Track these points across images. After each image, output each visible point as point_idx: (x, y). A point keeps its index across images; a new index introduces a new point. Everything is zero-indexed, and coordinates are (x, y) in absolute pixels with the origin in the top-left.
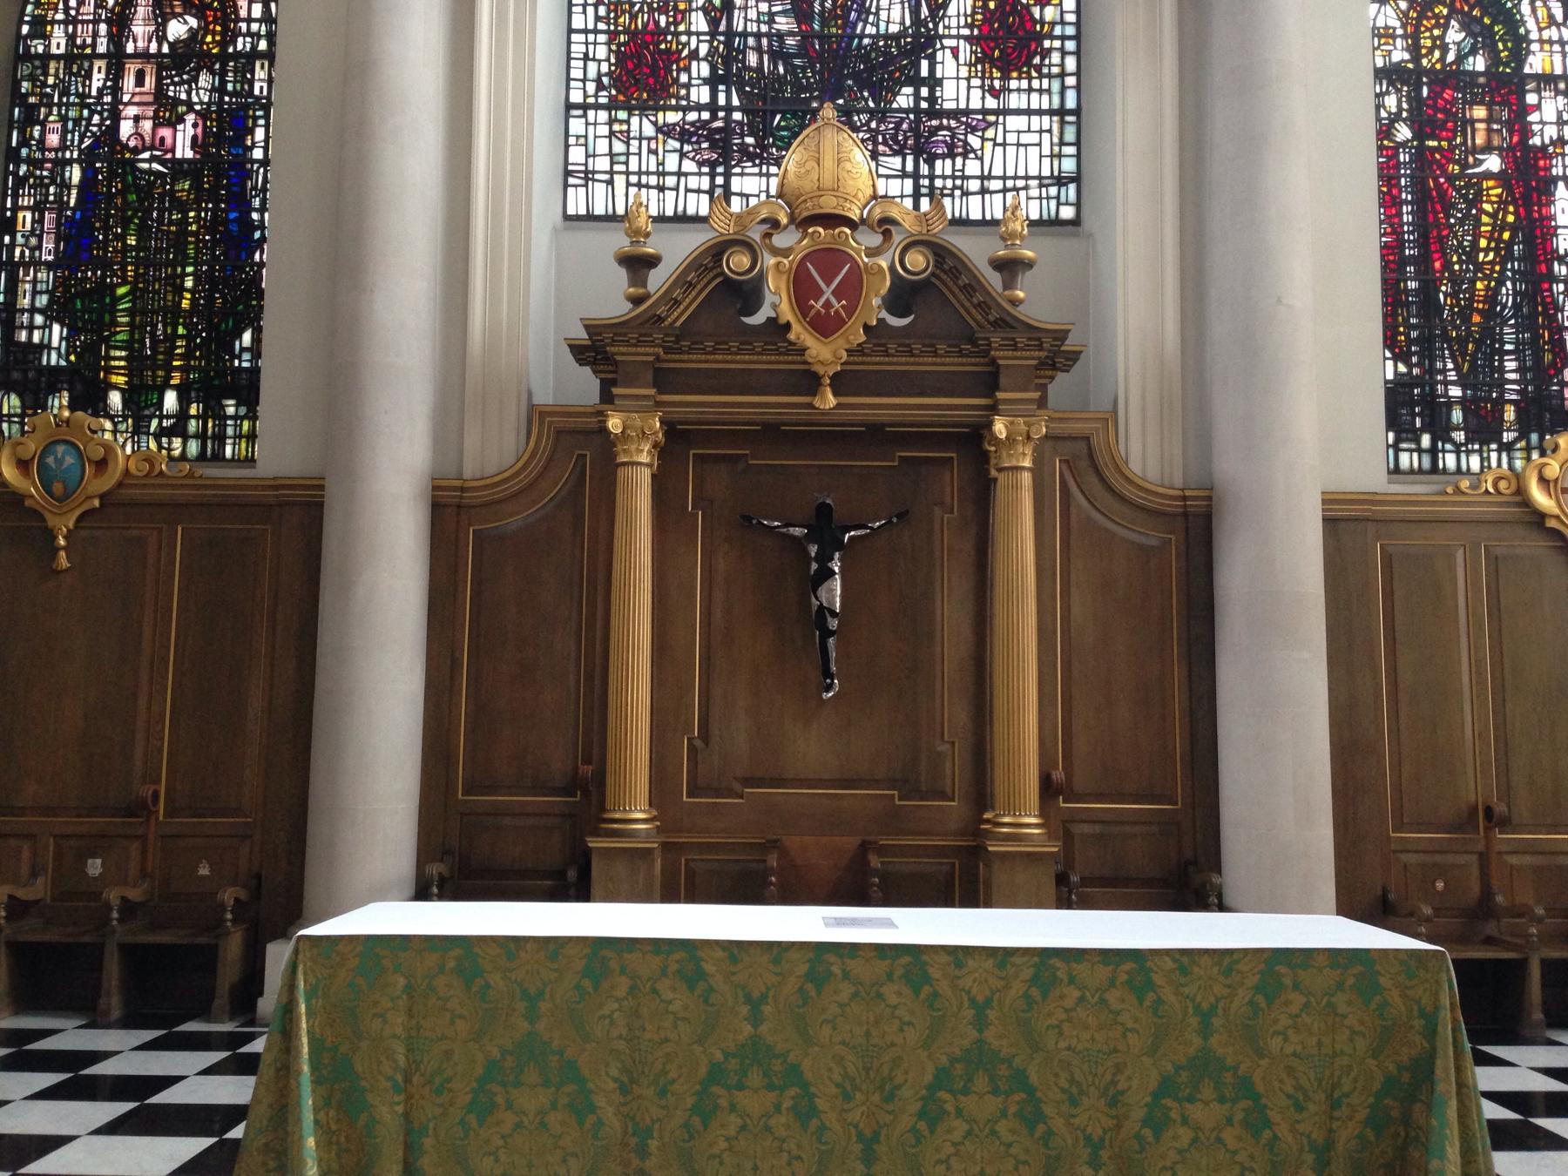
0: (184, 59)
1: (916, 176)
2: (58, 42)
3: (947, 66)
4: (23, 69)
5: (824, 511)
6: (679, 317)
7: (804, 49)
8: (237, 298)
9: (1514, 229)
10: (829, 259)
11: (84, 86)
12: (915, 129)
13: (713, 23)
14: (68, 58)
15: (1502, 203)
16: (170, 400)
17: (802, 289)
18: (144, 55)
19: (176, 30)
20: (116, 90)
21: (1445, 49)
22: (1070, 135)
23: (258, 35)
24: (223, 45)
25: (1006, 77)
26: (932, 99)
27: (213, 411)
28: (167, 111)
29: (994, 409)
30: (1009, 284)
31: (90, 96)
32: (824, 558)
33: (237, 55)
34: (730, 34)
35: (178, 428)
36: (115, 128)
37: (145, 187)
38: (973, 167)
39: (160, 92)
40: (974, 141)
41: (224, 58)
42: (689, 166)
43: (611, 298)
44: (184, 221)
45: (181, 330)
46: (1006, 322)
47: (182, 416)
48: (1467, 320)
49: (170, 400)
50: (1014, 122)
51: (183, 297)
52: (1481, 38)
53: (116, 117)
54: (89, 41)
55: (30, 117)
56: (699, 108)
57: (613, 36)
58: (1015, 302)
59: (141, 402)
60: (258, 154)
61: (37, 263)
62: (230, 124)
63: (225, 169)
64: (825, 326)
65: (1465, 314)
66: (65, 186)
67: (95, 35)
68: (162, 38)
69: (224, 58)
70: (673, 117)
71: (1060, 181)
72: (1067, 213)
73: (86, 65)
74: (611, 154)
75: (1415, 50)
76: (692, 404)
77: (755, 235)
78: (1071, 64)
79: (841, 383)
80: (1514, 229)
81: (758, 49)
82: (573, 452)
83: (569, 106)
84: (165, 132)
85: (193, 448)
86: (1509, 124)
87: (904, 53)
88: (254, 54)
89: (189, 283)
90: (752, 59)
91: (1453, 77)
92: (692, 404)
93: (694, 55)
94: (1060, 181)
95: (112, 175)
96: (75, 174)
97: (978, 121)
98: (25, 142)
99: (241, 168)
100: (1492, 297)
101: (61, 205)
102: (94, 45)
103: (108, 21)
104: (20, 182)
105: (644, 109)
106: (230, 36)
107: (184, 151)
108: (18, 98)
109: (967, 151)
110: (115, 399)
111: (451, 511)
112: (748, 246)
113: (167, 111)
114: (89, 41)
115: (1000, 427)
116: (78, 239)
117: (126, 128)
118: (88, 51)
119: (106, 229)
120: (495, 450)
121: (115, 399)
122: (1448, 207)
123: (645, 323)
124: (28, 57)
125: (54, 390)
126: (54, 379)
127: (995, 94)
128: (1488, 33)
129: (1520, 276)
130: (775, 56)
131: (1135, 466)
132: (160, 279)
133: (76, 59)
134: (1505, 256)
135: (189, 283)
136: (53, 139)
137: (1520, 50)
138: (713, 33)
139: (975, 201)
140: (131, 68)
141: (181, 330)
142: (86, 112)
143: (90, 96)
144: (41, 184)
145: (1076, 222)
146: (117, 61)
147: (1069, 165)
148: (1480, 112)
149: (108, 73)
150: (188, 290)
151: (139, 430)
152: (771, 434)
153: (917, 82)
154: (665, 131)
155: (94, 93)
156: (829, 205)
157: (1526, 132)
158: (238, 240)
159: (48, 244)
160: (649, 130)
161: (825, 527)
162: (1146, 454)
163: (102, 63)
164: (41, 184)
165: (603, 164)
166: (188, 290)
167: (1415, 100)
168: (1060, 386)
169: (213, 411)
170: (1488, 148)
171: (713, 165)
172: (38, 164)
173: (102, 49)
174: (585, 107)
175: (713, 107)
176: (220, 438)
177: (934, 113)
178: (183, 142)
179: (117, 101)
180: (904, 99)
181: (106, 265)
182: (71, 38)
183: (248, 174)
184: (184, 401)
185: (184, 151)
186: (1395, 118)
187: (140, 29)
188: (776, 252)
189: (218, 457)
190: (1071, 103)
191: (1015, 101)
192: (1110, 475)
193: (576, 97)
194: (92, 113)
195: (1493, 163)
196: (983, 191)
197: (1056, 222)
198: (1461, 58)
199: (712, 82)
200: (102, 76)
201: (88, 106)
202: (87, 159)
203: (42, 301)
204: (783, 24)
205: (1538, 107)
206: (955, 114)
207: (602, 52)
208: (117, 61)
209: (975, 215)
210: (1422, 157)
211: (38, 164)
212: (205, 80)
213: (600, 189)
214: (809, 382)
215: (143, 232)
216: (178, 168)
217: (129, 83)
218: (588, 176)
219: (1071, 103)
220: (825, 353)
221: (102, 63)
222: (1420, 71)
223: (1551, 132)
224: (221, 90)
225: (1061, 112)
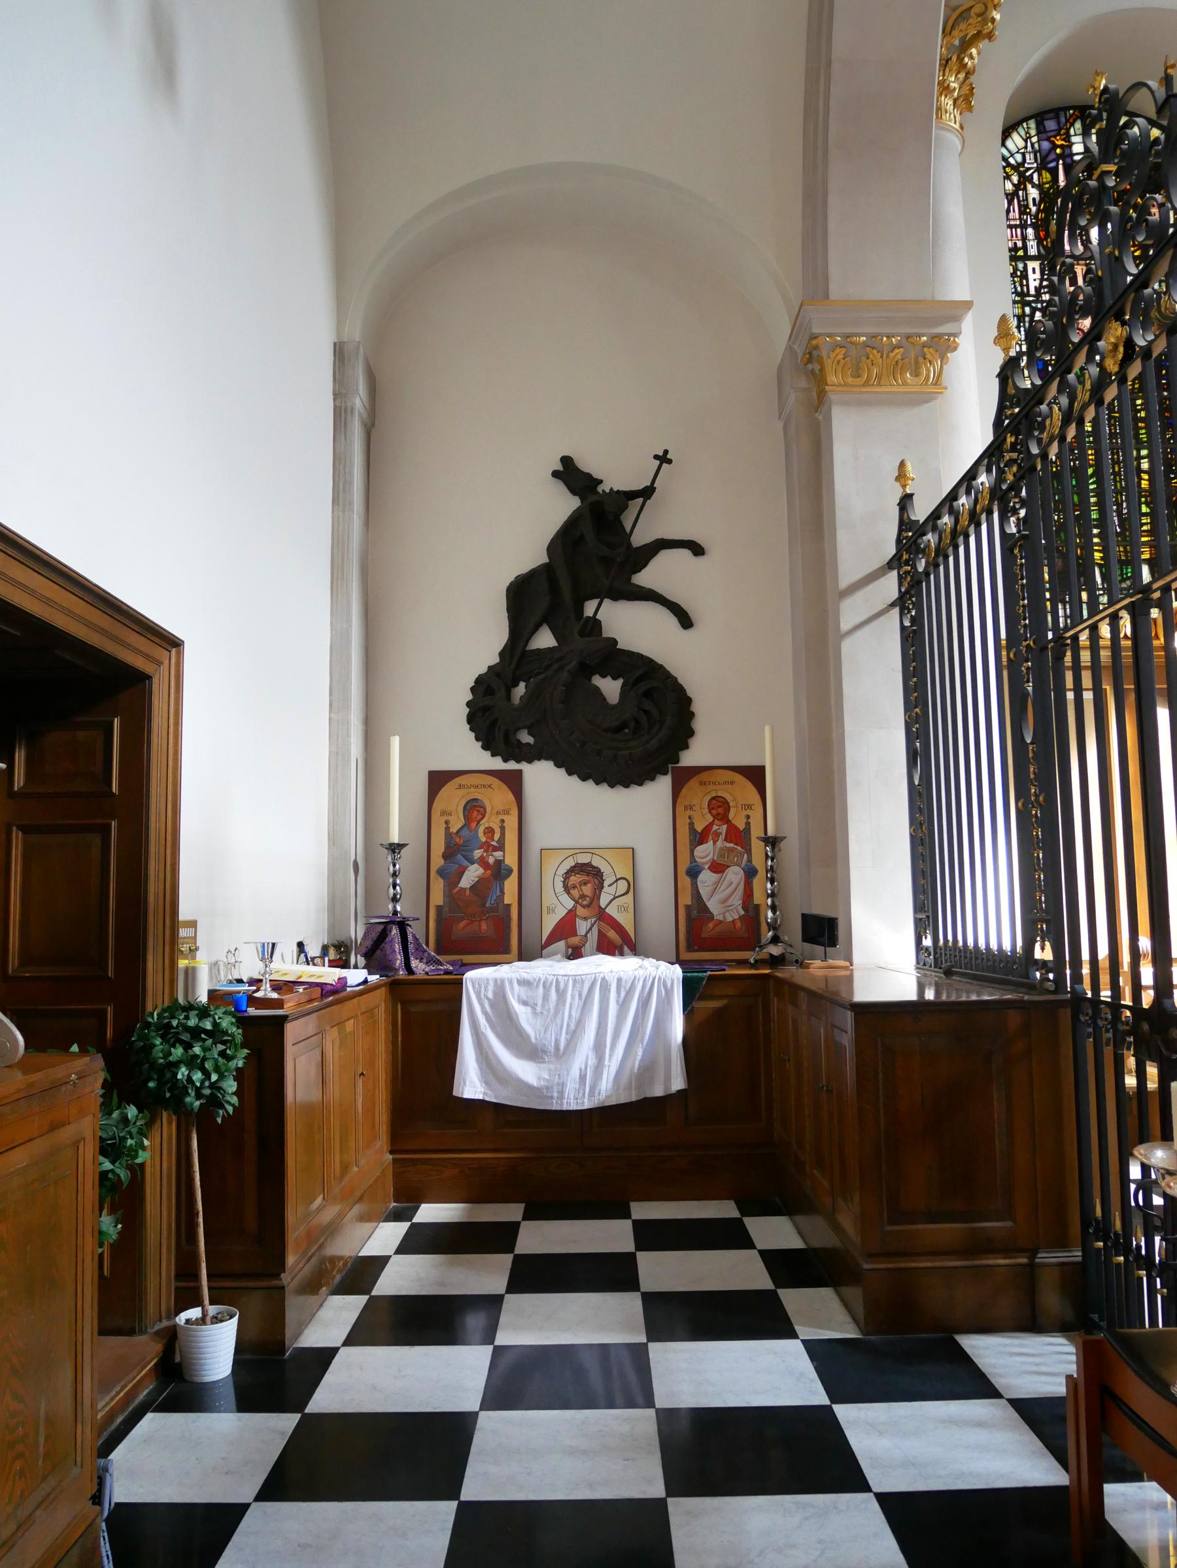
11: (1022, 285)
31: (1028, 295)
45: (1144, 509)
51: (1140, 479)
54: (1020, 244)
67: (1024, 238)
73: (1021, 266)
89: (1145, 465)
102: (1025, 248)
103: (1033, 225)
114: (1020, 244)
118: (1021, 253)
132: (1118, 462)
135: (1145, 465)
141: (1144, 509)
142: (1027, 310)
143: (1028, 295)
149: (1042, 274)
150: (1145, 472)
155: (1032, 292)
163: (1036, 264)
166: (1145, 472)
173: (1033, 251)
194: (1034, 310)
200: (1038, 275)
201: (1028, 304)
221: (1036, 264)
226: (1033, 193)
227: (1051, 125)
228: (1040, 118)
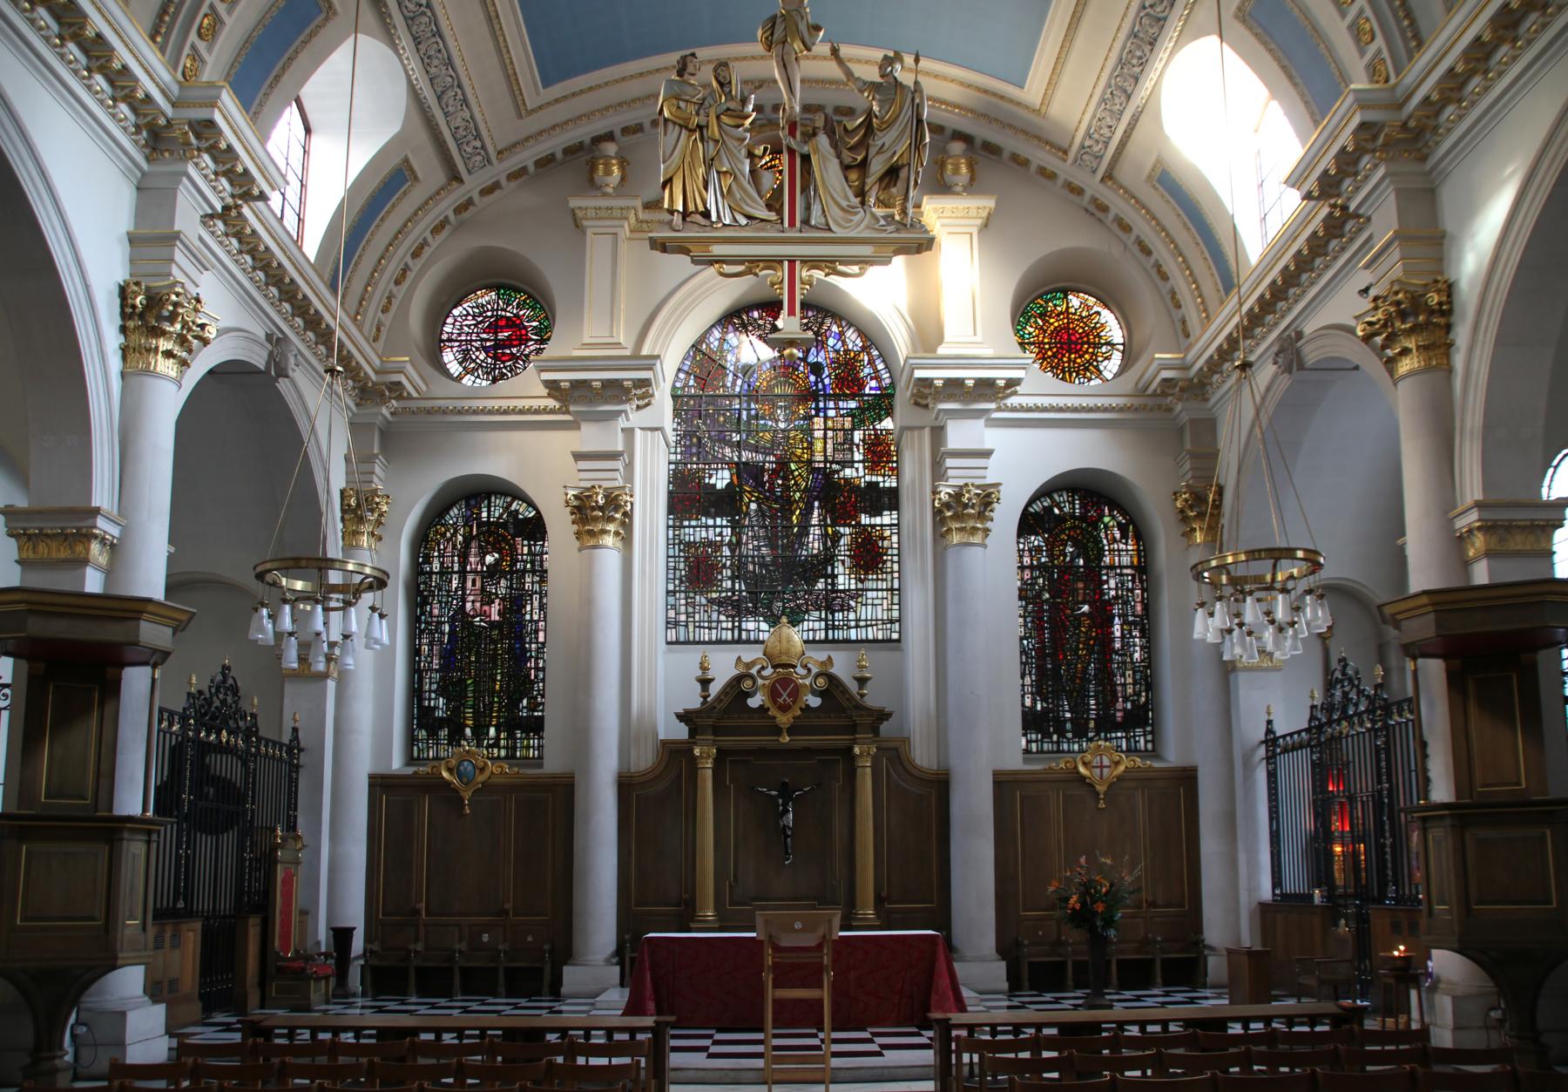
0: (493, 573)
1: (826, 620)
2: (436, 566)
3: (840, 569)
4: (422, 579)
5: (784, 785)
6: (722, 706)
7: (774, 562)
8: (521, 684)
9: (1095, 639)
10: (785, 682)
12: (826, 598)
13: (733, 551)
14: (441, 573)
15: (1090, 628)
16: (492, 731)
17: (774, 693)
18: (475, 572)
19: (489, 559)
20: (464, 589)
21: (1065, 555)
22: (896, 600)
23: (525, 562)
24: (511, 566)
25: (866, 573)
26: (833, 584)
27: (511, 736)
28: (487, 599)
29: (855, 741)
30: (861, 688)
32: (785, 805)
33: (517, 571)
34: (741, 556)
35: (496, 745)
36: (464, 606)
37: (478, 634)
38: (852, 616)
39: (483, 589)
40: (852, 603)
41: (512, 572)
42: (723, 618)
43: (695, 703)
44: (496, 649)
46: (859, 707)
47: (498, 738)
48: (1073, 682)
49: (492, 731)
50: (870, 594)
52: (1081, 550)
53: (464, 601)
55: (425, 602)
56: (727, 590)
57: (687, 558)
58: (862, 696)
59: (480, 732)
60: (528, 617)
61: (431, 670)
62: (515, 603)
63: (514, 626)
64: (784, 708)
65: (1073, 680)
66: (443, 633)
68: (483, 564)
69: (512, 572)
70: (714, 595)
71: (891, 622)
72: (895, 636)
74: (687, 613)
75: (1051, 556)
76: (729, 741)
77: (754, 671)
78: (896, 567)
79: (792, 731)
80: (1095, 639)
81: (754, 563)
82: (675, 756)
83: (668, 592)
84: (486, 608)
85: (503, 753)
86: (1094, 591)
87: (820, 563)
88: (525, 571)
90: (751, 567)
91: (1069, 568)
92: (729, 741)
93: (724, 566)
94: (891, 622)
95: (463, 628)
96: (447, 628)
97: (857, 594)
98: (423, 613)
99: (521, 624)
100: (1085, 670)
101: (442, 643)
104: (422, 632)
105: (701, 594)
106: (514, 562)
107: (495, 617)
108: (420, 593)
109: (849, 608)
110: (468, 731)
111: (626, 786)
112: (751, 677)
113: (487, 599)
115: (857, 750)
116: (447, 657)
117: (469, 606)
119: (461, 653)
120: (644, 760)
121: (468, 731)
122: (1066, 630)
123: (707, 709)
124: (422, 573)
125: (441, 728)
126: (441, 723)
127: (862, 581)
128: (1085, 547)
129: (1097, 661)
130: (763, 565)
131: (918, 761)
133: (445, 572)
134: (1090, 651)
136: (436, 612)
137: (1100, 554)
138: (732, 557)
139: (853, 631)
140: (470, 578)
144: (431, 632)
145: (898, 641)
146: (463, 574)
147: (896, 614)
148: (1081, 585)
151: (479, 745)
152: (762, 752)
153: (826, 576)
154: (711, 601)
156: (784, 660)
157: (1102, 593)
158: (520, 656)
159: (436, 661)
160: (704, 601)
161: (786, 791)
162: (923, 756)
164: (431, 632)
165: (683, 618)
167: (1051, 579)
168: (884, 727)
169: (511, 736)
170: (1084, 603)
171: (733, 617)
172: (429, 624)
174: (674, 592)
175: (733, 590)
176: (514, 748)
177: (834, 591)
178: (494, 612)
179: (464, 593)
180: (820, 585)
181: (461, 670)
182: (442, 564)
183: (524, 626)
184: (498, 732)
185: (495, 617)
186: (1042, 589)
187: (472, 559)
188: (763, 678)
189: (514, 756)
190: (896, 586)
191: (870, 585)
192: (909, 767)
193: (671, 587)
195: (1086, 608)
196: (857, 627)
197: (891, 641)
198: (1072, 559)
199: (733, 578)
202: (452, 620)
203: (434, 687)
204: (764, 550)
205: (1107, 582)
206: (843, 591)
207: (682, 566)
208: (463, 574)
209: (853, 637)
210: (1053, 606)
211: (429, 624)
212: (503, 583)
213: (682, 629)
214: (777, 731)
215: (478, 654)
216: (492, 624)
217: (469, 584)
218: (676, 624)
219: (896, 586)
220: (784, 720)
222: (1054, 567)
223: (1113, 593)
224: (511, 587)
225: (892, 589)
226: (460, 538)
227: (473, 502)
228: (467, 498)
